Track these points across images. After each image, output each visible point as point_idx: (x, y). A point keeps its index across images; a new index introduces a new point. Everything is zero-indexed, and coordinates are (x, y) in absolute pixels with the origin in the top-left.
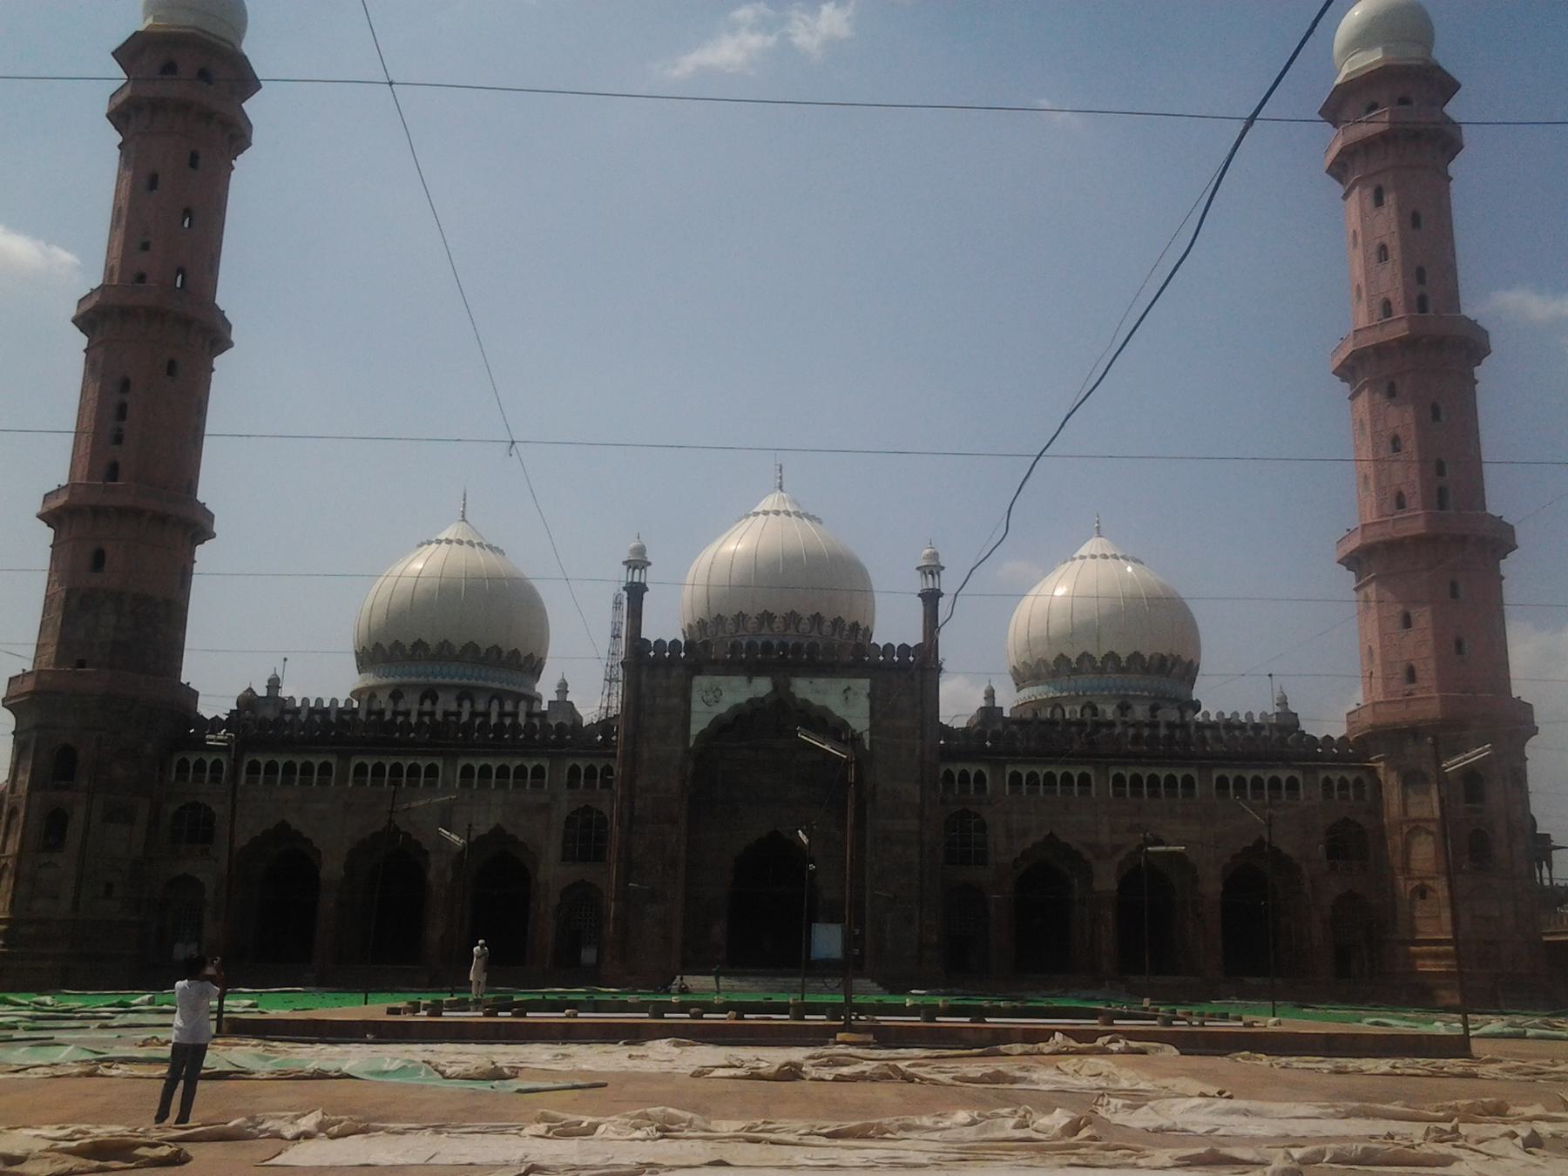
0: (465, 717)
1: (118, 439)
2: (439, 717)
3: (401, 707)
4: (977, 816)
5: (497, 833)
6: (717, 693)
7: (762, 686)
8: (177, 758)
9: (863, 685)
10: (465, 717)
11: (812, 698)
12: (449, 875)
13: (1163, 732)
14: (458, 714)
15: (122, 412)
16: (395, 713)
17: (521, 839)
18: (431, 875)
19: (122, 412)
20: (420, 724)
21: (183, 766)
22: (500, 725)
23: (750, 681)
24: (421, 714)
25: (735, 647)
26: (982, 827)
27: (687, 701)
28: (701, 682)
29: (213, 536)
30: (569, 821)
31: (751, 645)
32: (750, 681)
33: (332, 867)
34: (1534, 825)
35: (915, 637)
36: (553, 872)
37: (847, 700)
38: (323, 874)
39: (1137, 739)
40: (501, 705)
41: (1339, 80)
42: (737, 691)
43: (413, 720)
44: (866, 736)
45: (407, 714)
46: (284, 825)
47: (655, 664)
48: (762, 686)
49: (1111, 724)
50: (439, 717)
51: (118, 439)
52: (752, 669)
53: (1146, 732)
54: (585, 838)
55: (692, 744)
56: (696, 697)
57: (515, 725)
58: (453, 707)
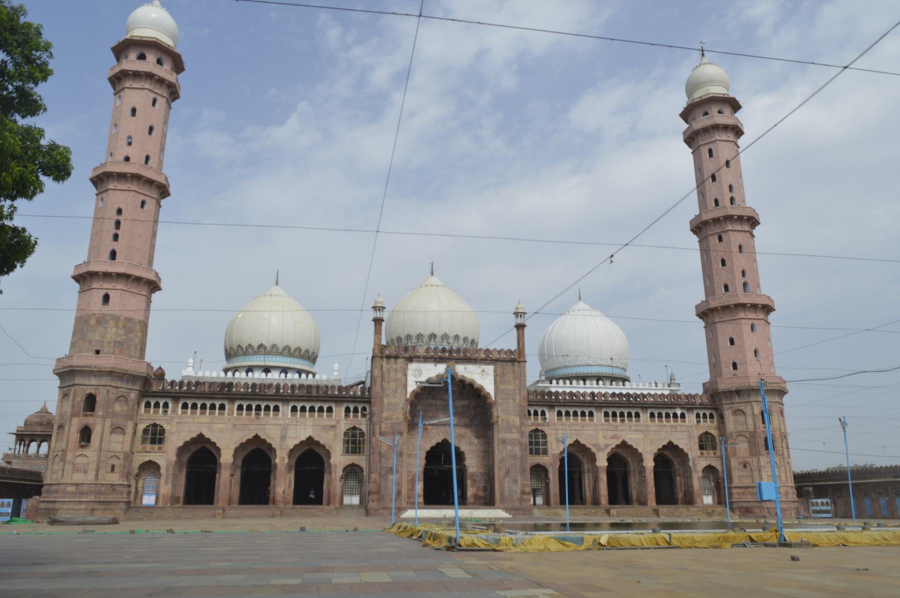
4: (542, 431)
5: (310, 439)
6: (420, 372)
9: (490, 369)
11: (466, 375)
12: (286, 460)
17: (322, 442)
18: (277, 461)
26: (545, 436)
27: (406, 375)
28: (413, 367)
30: (346, 434)
31: (435, 349)
33: (226, 457)
35: (514, 347)
36: (339, 459)
37: (484, 377)
42: (432, 371)
46: (201, 436)
47: (388, 357)
48: (441, 368)
52: (438, 360)
54: (354, 441)
55: (408, 396)
56: (410, 373)
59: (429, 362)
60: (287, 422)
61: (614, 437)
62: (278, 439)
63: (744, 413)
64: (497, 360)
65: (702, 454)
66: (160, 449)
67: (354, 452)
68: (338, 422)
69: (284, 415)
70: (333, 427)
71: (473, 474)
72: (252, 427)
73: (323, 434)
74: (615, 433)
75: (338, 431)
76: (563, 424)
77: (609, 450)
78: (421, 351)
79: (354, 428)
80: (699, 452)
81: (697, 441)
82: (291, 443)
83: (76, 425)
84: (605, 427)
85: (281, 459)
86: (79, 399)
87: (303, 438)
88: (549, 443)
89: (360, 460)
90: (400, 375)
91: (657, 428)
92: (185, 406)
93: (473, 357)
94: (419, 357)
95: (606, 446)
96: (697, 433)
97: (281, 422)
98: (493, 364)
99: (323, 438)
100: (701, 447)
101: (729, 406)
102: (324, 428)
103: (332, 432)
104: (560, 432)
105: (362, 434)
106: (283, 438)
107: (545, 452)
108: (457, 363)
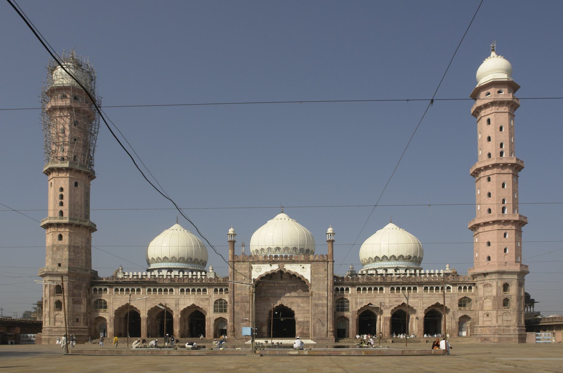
0: (181, 276)
1: (61, 204)
2: (173, 277)
3: (161, 274)
7: (275, 267)
8: (93, 288)
9: (308, 266)
10: (181, 276)
13: (408, 275)
14: (179, 276)
15: (62, 197)
16: (159, 276)
18: (174, 316)
19: (62, 197)
20: (167, 278)
21: (95, 290)
22: (192, 278)
23: (271, 265)
24: (167, 276)
25: (265, 257)
29: (96, 230)
30: (216, 302)
32: (271, 265)
33: (144, 315)
34: (530, 297)
36: (211, 316)
38: (141, 316)
39: (399, 278)
40: (192, 273)
41: (477, 86)
42: (266, 269)
43: (165, 277)
44: (309, 279)
45: (163, 276)
49: (391, 274)
50: (173, 277)
51: (61, 204)
52: (271, 262)
53: (403, 276)
54: (220, 306)
57: (197, 279)
58: (177, 273)
59: (266, 264)
60: (178, 297)
61: (396, 301)
62: (174, 306)
63: (491, 286)
64: (313, 261)
65: (460, 309)
66: (105, 311)
67: (221, 311)
68: (210, 296)
69: (176, 293)
70: (207, 299)
71: (300, 322)
72: (157, 300)
73: (201, 303)
74: (398, 299)
75: (211, 301)
76: (361, 295)
77: (393, 308)
78: (261, 258)
79: (221, 299)
80: (458, 308)
81: (457, 302)
82: (182, 308)
83: (53, 299)
84: (391, 296)
85: (176, 316)
86: (52, 288)
87: (189, 304)
88: (350, 306)
89: (227, 316)
90: (247, 271)
91: (428, 296)
92: (117, 290)
93: (297, 259)
94: (259, 261)
95: (391, 306)
96: (457, 298)
97: (175, 297)
98: (310, 263)
99: (201, 305)
100: (460, 305)
101: (482, 282)
102: (202, 300)
103: (207, 302)
104: (358, 299)
105: (227, 303)
106: (177, 305)
107: (348, 310)
108: (285, 263)
